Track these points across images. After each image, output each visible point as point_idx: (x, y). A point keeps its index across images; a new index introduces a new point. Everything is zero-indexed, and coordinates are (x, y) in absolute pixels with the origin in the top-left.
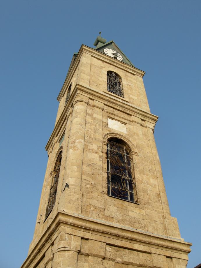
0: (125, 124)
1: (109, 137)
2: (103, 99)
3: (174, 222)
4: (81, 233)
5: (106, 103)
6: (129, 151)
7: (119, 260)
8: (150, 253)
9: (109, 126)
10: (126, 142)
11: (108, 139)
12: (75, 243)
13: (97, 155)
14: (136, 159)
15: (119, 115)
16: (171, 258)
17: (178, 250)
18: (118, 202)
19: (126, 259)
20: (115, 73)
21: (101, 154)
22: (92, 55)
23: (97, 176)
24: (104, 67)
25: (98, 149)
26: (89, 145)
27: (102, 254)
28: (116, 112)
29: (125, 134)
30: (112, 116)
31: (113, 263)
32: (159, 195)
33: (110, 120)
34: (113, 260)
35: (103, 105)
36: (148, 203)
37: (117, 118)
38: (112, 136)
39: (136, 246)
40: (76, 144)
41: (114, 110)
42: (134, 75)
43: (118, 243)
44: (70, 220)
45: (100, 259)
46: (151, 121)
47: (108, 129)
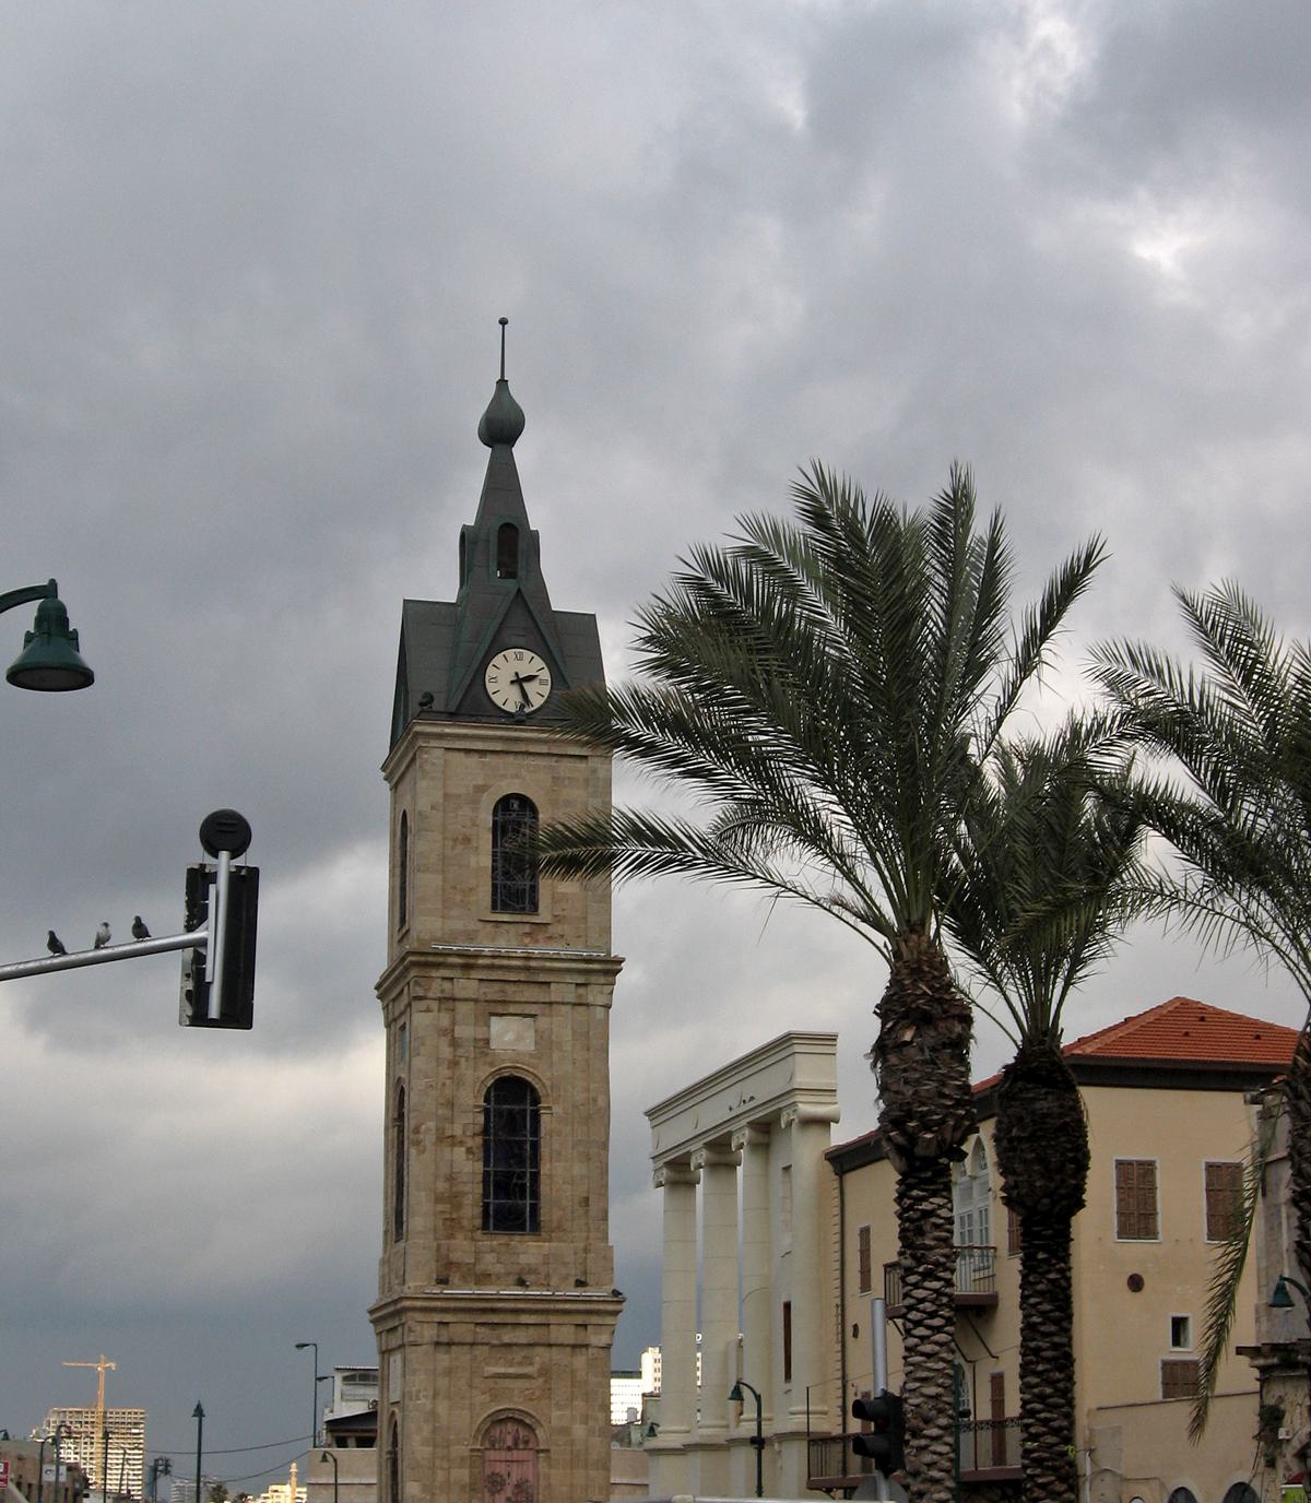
4: (437, 1317)
7: (495, 1342)
8: (549, 1325)
9: (493, 1046)
10: (530, 1079)
12: (429, 1333)
13: (463, 1149)
16: (585, 1326)
18: (499, 1240)
19: (506, 1339)
21: (470, 1142)
24: (480, 789)
25: (464, 1133)
28: (510, 989)
31: (486, 1348)
32: (586, 1200)
33: (493, 1019)
34: (487, 1344)
36: (559, 1227)
37: (512, 1009)
38: (497, 1077)
39: (524, 1319)
40: (421, 1136)
42: (585, 757)
43: (495, 1319)
44: (419, 1304)
46: (602, 980)
47: (488, 1059)
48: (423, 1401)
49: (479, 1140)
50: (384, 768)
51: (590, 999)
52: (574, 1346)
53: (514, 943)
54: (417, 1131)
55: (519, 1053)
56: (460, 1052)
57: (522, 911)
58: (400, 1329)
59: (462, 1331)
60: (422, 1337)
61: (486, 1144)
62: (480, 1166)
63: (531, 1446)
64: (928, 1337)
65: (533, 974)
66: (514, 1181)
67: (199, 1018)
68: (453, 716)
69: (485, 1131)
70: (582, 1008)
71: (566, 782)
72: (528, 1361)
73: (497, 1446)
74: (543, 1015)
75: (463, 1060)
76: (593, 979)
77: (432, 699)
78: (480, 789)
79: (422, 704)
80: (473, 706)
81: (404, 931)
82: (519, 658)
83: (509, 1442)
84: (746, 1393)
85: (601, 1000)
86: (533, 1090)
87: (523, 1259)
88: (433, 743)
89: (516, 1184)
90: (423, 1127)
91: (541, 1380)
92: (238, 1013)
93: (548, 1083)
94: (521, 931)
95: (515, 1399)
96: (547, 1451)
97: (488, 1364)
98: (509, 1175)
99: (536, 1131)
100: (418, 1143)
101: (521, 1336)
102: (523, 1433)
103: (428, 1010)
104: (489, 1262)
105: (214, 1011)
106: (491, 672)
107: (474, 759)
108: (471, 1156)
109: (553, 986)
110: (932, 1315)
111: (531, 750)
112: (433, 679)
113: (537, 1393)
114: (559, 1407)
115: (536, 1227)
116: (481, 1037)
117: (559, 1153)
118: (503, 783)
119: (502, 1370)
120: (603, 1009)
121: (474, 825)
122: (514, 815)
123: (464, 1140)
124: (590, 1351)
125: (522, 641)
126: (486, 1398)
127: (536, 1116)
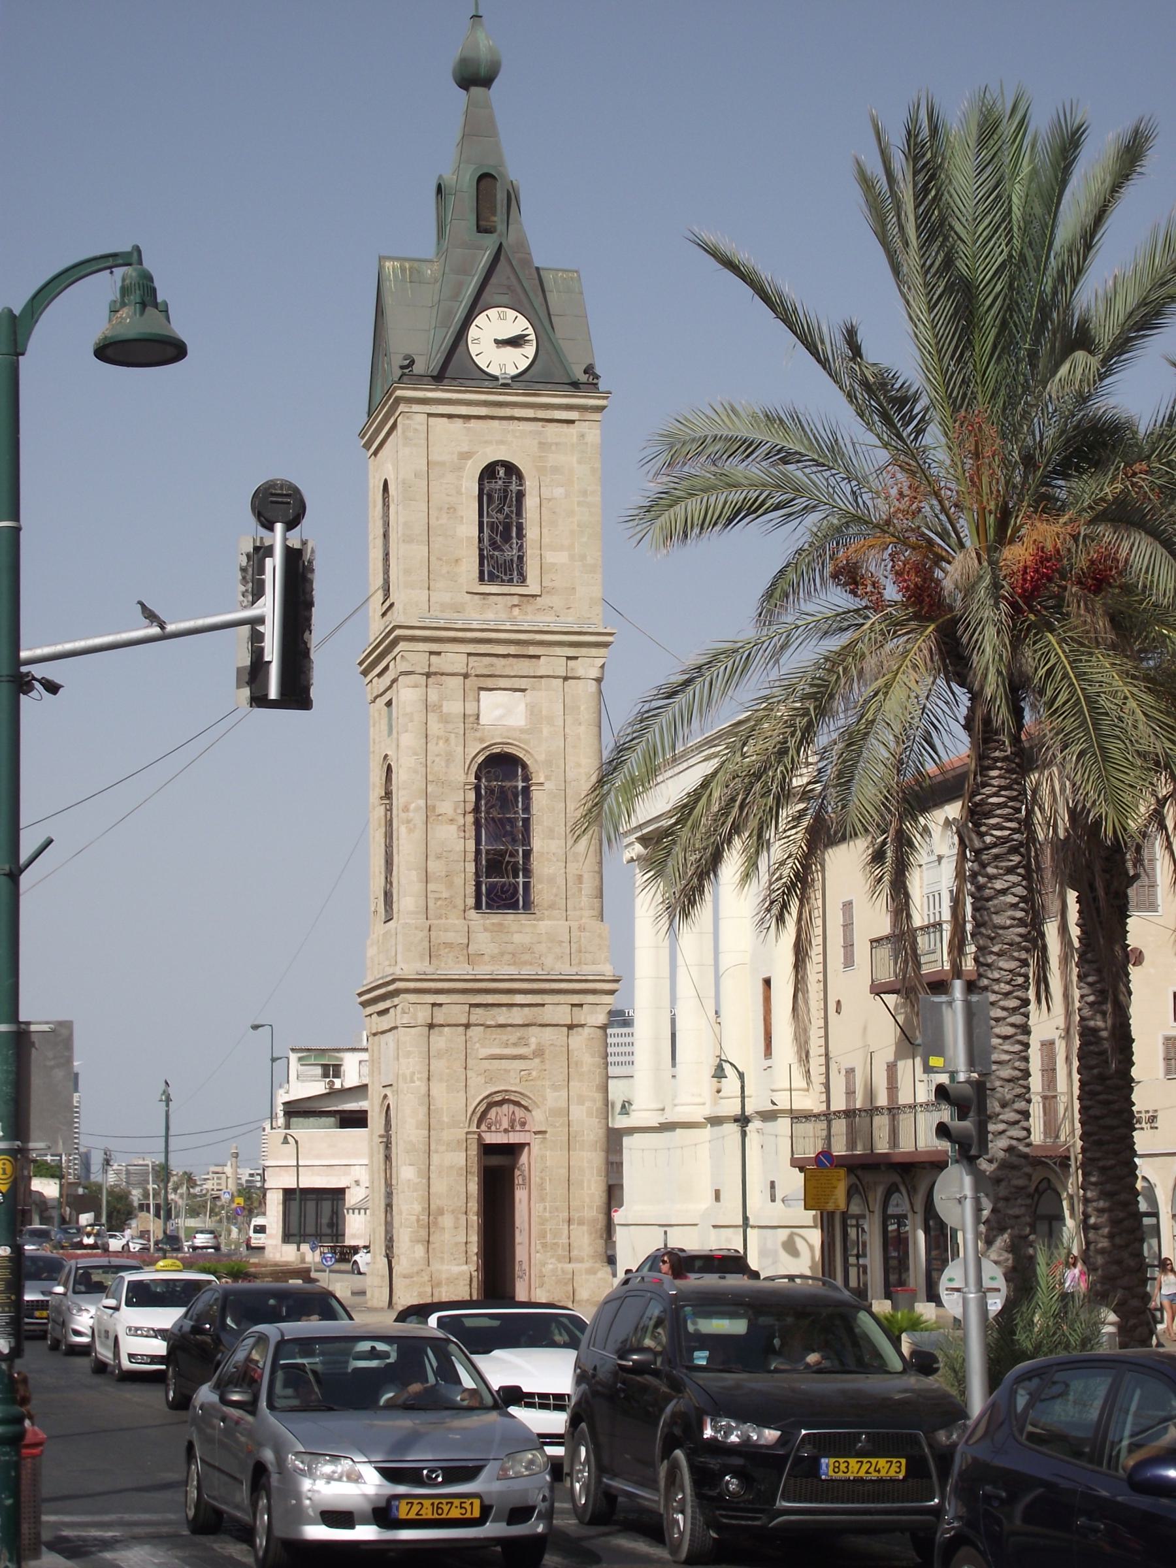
0: (523, 690)
3: (600, 936)
6: (527, 778)
9: (483, 721)
10: (521, 756)
12: (423, 1015)
14: (539, 799)
16: (581, 1005)
17: (594, 992)
19: (502, 1021)
25: (455, 810)
26: (438, 803)
27: (464, 1021)
28: (500, 665)
30: (489, 683)
31: (482, 1028)
33: (482, 693)
36: (552, 906)
39: (519, 999)
40: (411, 815)
41: (494, 660)
42: (572, 422)
44: (412, 985)
45: (461, 1029)
46: (594, 651)
47: (478, 734)
48: (418, 1083)
49: (470, 818)
50: (362, 435)
51: (580, 672)
52: (570, 1027)
53: (504, 616)
54: (406, 809)
56: (450, 727)
57: (511, 580)
58: (392, 1010)
59: (454, 1009)
60: (416, 1019)
61: (477, 823)
62: (471, 845)
63: (527, 1128)
64: (1005, 1019)
65: (525, 647)
66: (507, 858)
67: (259, 700)
68: (439, 378)
69: (477, 810)
71: (553, 447)
72: (523, 1042)
73: (493, 1128)
74: (534, 689)
75: (453, 735)
76: (583, 651)
77: (413, 362)
78: (466, 456)
79: (402, 367)
80: (453, 367)
81: (387, 604)
82: (502, 318)
83: (505, 1125)
84: (726, 1066)
85: (595, 673)
86: (525, 766)
87: (517, 938)
88: (416, 408)
89: (508, 862)
91: (537, 1060)
92: (296, 694)
94: (510, 604)
95: (510, 1080)
96: (544, 1132)
97: (483, 1046)
98: (502, 854)
99: (527, 809)
100: (409, 821)
101: (517, 1016)
102: (520, 1113)
103: (416, 686)
104: (483, 942)
105: (273, 694)
106: (473, 332)
107: (459, 423)
108: (462, 834)
110: (1007, 995)
111: (517, 415)
112: (417, 339)
113: (534, 1073)
114: (555, 1088)
115: (528, 906)
117: (551, 830)
119: (498, 1051)
121: (459, 493)
122: (500, 482)
124: (587, 1030)
125: (505, 299)
126: (481, 1080)
127: (526, 791)
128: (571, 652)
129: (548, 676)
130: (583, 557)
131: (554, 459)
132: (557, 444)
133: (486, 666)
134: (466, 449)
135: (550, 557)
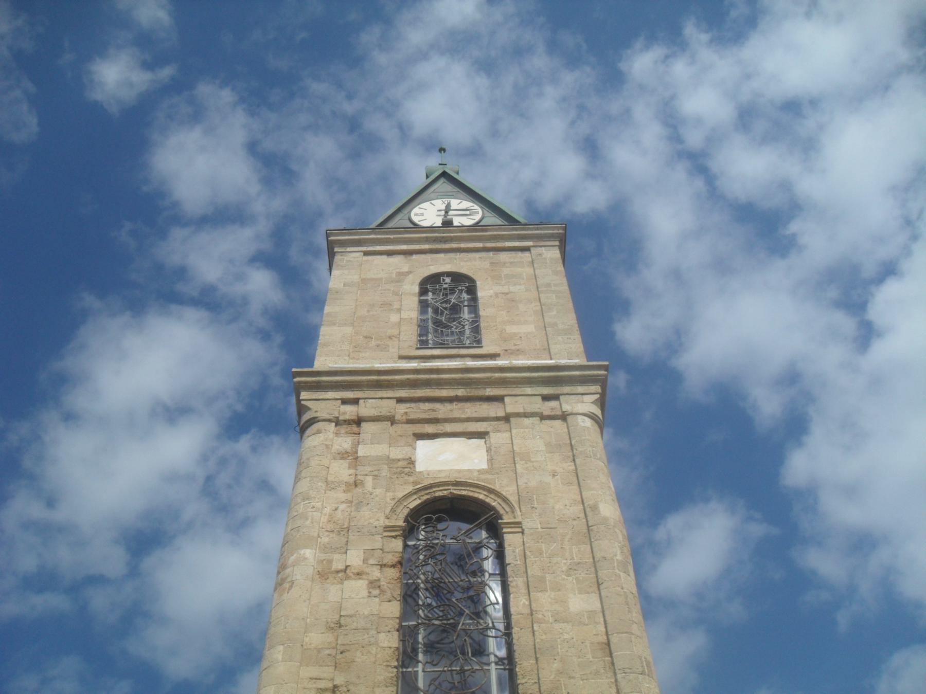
0: (481, 435)
1: (412, 506)
2: (389, 385)
5: (403, 393)
9: (420, 467)
10: (481, 497)
11: (412, 510)
15: (456, 414)
20: (449, 274)
21: (376, 573)
22: (365, 249)
23: (358, 654)
24: (409, 273)
25: (365, 561)
29: (476, 474)
30: (430, 429)
33: (420, 444)
35: (393, 402)
37: (449, 428)
38: (425, 498)
41: (438, 406)
46: (580, 389)
47: (411, 479)
51: (566, 407)
55: (459, 471)
62: (394, 609)
70: (557, 423)
76: (567, 389)
90: (293, 558)
93: (513, 499)
108: (376, 592)
109: (507, 399)
116: (400, 457)
117: (542, 580)
118: (431, 267)
120: (586, 419)
123: (367, 570)
128: (547, 391)
129: (518, 415)
130: (555, 324)
131: (506, 271)
132: (511, 263)
133: (425, 411)
134: (406, 269)
135: (511, 329)
